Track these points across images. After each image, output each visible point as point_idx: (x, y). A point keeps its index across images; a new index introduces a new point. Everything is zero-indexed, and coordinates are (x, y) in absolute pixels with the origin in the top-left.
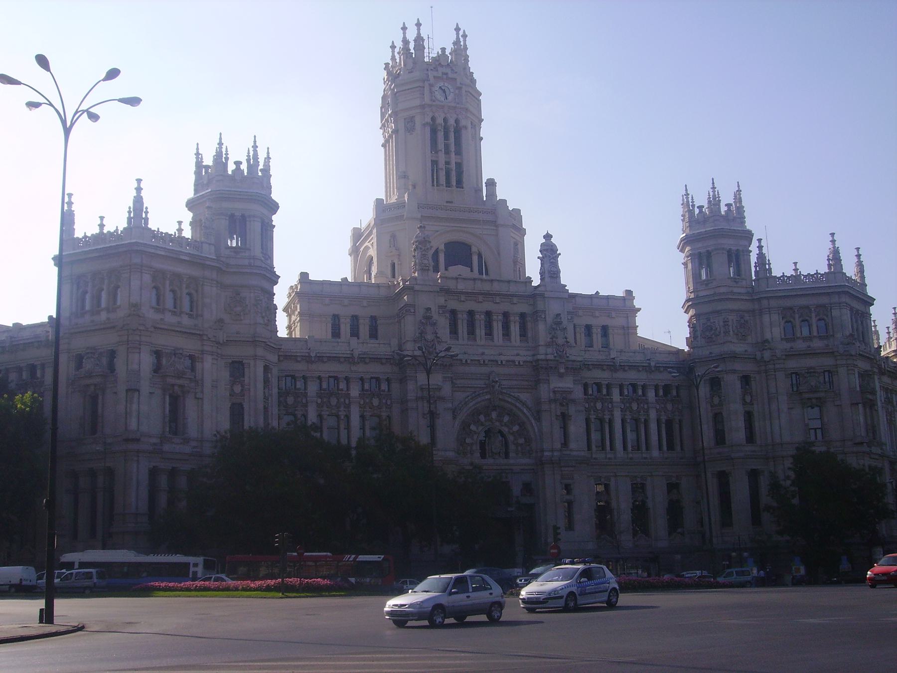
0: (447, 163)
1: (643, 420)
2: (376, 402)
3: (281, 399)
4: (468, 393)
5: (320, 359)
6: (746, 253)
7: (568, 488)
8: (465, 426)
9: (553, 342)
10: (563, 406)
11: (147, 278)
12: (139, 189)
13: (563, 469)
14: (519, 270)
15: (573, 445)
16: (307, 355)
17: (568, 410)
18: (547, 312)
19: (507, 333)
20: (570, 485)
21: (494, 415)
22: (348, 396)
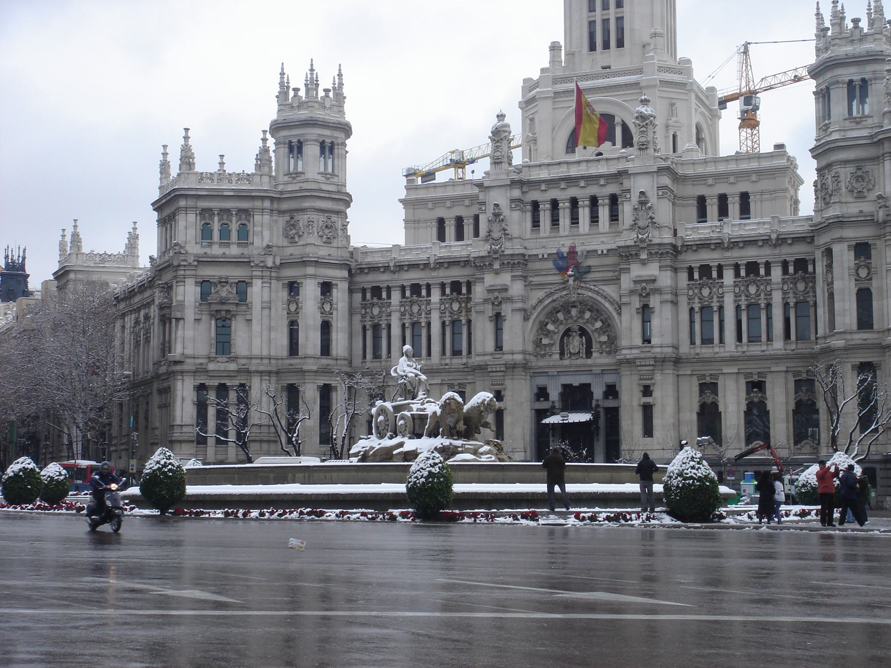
0: (606, 22)
1: (763, 305)
2: (456, 307)
3: (368, 310)
4: (546, 290)
5: (400, 267)
6: (873, 82)
7: (647, 391)
8: (543, 326)
9: (635, 224)
10: (644, 297)
11: (192, 217)
12: (186, 138)
13: (639, 368)
14: (674, 137)
15: (655, 341)
16: (387, 265)
18: (632, 191)
19: (594, 219)
20: (649, 386)
21: (574, 312)
22: (429, 303)
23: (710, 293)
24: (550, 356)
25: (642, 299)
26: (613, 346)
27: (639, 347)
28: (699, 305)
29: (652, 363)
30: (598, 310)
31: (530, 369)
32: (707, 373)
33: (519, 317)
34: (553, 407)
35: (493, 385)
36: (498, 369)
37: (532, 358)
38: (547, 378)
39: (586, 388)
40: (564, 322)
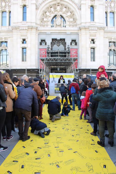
13: (90, 31)
17: (95, 3)
21: (58, 8)
23: (114, 6)
24: (47, 26)
25: (92, 2)
26: (75, 23)
27: (90, 22)
28: (110, 10)
29: (96, 29)
30: (68, 8)
31: (38, 30)
32: (113, 37)
33: (34, 7)
34: (48, 48)
35: (21, 36)
36: (24, 29)
37: (39, 26)
38: (45, 35)
39: (63, 41)
40: (54, 12)
